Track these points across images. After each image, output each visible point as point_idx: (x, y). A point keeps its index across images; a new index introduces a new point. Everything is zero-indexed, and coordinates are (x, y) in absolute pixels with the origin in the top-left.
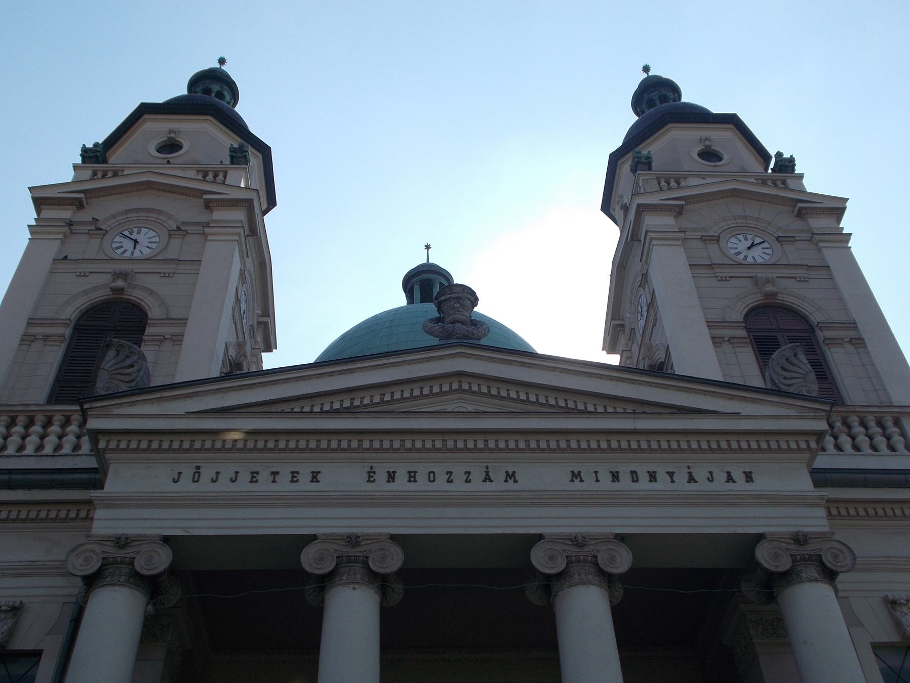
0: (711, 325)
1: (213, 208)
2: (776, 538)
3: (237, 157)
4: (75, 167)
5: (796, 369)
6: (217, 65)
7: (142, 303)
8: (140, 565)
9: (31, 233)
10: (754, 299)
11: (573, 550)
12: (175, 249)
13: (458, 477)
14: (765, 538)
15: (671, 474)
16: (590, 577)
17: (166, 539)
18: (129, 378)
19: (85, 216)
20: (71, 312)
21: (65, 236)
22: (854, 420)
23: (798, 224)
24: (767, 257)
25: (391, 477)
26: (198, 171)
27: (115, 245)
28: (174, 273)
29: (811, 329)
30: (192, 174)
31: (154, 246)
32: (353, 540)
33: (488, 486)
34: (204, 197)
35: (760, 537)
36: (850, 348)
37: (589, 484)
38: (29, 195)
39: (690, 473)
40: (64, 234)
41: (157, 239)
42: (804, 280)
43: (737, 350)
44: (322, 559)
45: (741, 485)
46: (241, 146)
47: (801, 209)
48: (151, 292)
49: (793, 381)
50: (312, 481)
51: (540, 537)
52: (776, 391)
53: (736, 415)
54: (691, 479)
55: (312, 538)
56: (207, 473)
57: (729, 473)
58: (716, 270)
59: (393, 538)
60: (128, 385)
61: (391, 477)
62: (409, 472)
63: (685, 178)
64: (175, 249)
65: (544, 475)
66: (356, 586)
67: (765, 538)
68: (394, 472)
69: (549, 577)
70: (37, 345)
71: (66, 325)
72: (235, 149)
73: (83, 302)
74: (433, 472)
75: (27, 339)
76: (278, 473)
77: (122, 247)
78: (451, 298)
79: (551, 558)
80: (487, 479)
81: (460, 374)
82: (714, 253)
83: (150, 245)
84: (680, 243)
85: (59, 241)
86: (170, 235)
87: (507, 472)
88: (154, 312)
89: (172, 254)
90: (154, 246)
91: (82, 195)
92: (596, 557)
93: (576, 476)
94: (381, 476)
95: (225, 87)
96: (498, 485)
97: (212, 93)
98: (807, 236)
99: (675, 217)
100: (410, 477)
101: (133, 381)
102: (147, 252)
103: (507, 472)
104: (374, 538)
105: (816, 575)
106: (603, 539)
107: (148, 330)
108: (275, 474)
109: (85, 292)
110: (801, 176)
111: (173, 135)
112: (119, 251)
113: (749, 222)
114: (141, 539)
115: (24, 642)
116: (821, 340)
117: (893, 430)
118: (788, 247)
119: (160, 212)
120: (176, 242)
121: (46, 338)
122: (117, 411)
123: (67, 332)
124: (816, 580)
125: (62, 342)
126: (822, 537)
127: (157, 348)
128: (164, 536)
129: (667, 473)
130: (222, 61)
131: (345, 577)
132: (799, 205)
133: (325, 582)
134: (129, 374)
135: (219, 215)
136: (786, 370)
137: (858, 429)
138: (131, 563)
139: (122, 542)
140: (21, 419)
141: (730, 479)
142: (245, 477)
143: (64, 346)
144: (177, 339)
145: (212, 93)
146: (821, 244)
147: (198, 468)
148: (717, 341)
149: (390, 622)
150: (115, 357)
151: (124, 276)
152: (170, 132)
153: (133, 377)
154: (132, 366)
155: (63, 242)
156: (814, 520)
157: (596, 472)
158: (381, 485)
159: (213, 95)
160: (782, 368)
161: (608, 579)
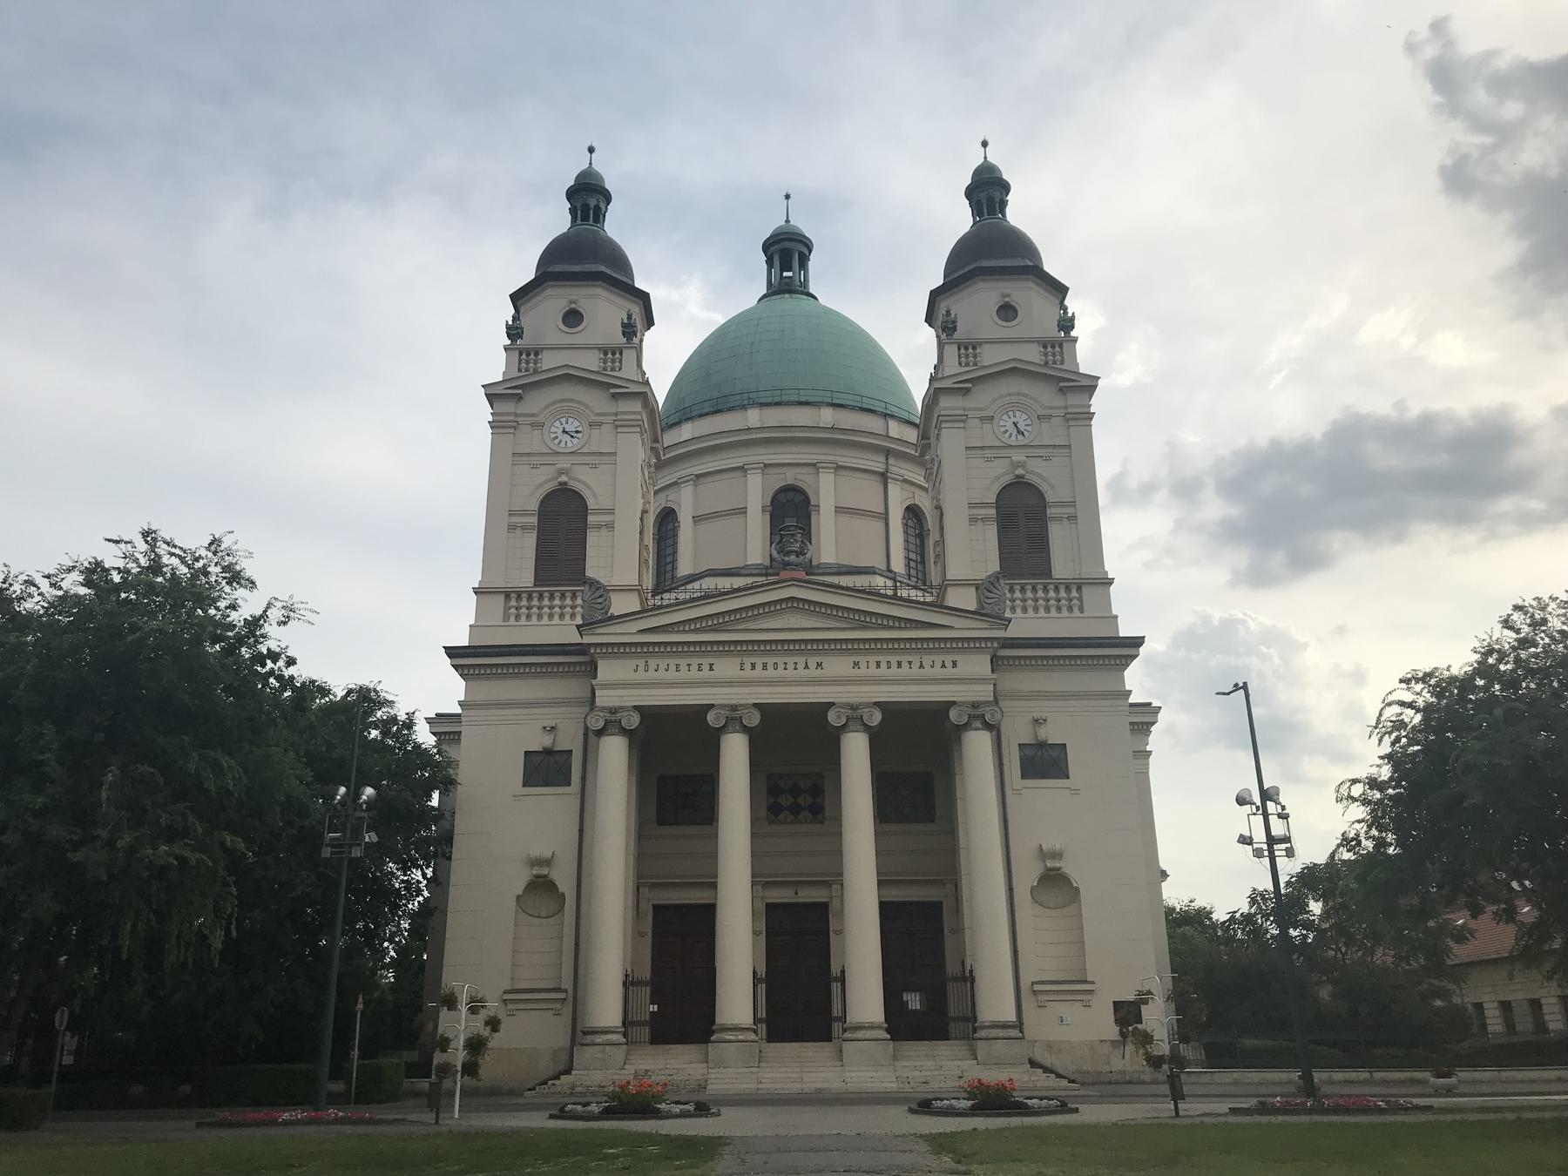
0: (972, 506)
2: (963, 704)
13: (791, 666)
17: (636, 708)
19: (523, 408)
23: (1058, 401)
32: (734, 708)
37: (863, 671)
42: (1048, 459)
45: (949, 671)
54: (921, 666)
55: (712, 706)
59: (755, 705)
61: (753, 666)
65: (838, 666)
70: (518, 531)
73: (541, 493)
75: (512, 527)
80: (806, 667)
81: (792, 599)
88: (591, 504)
93: (856, 664)
94: (748, 667)
98: (1062, 412)
104: (745, 706)
107: (591, 519)
109: (540, 485)
110: (1075, 340)
115: (562, 746)
118: (1045, 426)
119: (580, 403)
120: (595, 432)
121: (524, 528)
126: (987, 703)
133: (721, 730)
139: (613, 710)
141: (943, 666)
144: (610, 526)
156: (984, 693)
161: (867, 728)
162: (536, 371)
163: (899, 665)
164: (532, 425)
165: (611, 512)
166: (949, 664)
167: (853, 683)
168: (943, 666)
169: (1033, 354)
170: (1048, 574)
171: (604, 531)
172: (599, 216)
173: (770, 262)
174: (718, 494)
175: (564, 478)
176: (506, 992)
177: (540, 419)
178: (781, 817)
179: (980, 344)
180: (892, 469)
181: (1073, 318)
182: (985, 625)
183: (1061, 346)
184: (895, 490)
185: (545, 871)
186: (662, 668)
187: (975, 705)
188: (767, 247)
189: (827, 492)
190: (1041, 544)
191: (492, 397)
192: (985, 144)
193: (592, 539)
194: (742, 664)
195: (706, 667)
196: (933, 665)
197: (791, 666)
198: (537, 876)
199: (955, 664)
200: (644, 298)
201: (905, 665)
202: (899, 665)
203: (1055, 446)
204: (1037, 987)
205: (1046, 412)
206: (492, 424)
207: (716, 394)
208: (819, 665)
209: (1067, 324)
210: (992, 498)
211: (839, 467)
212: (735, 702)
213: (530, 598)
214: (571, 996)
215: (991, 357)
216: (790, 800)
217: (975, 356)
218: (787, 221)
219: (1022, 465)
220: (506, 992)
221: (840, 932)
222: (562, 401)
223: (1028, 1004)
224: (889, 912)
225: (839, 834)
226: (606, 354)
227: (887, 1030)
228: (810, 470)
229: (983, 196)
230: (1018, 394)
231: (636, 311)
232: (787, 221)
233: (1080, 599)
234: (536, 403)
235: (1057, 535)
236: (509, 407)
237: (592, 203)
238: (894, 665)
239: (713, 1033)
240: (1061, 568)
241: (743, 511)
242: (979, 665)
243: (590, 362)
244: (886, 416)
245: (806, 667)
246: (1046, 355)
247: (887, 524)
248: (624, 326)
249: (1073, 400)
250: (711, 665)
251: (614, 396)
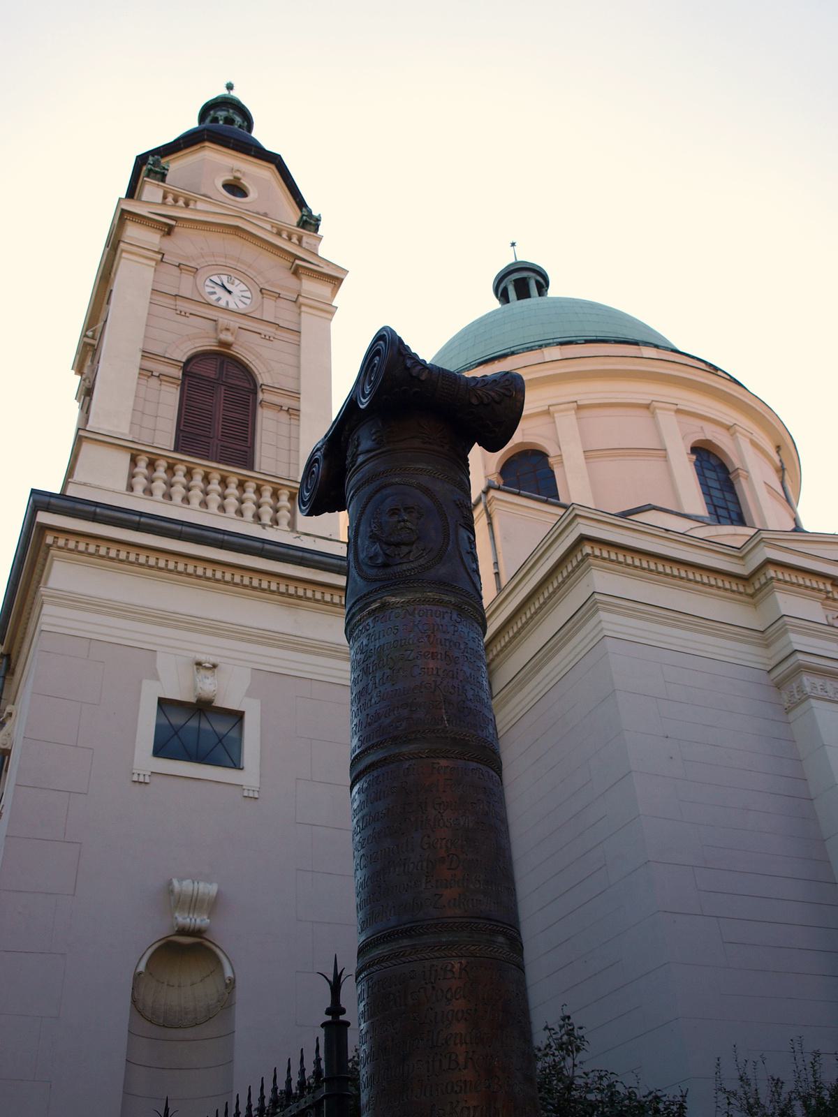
1: (303, 276)
6: (224, 92)
7: (251, 365)
12: (270, 310)
19: (168, 245)
26: (272, 227)
30: (268, 227)
31: (248, 301)
34: (298, 262)
41: (248, 294)
64: (270, 310)
70: (154, 382)
91: (173, 223)
97: (225, 124)
102: (242, 307)
111: (238, 175)
120: (269, 303)
130: (230, 87)
140: (162, 465)
145: (225, 124)
155: (155, 271)
159: (221, 122)
185: (199, 920)
198: (183, 931)
213: (171, 469)
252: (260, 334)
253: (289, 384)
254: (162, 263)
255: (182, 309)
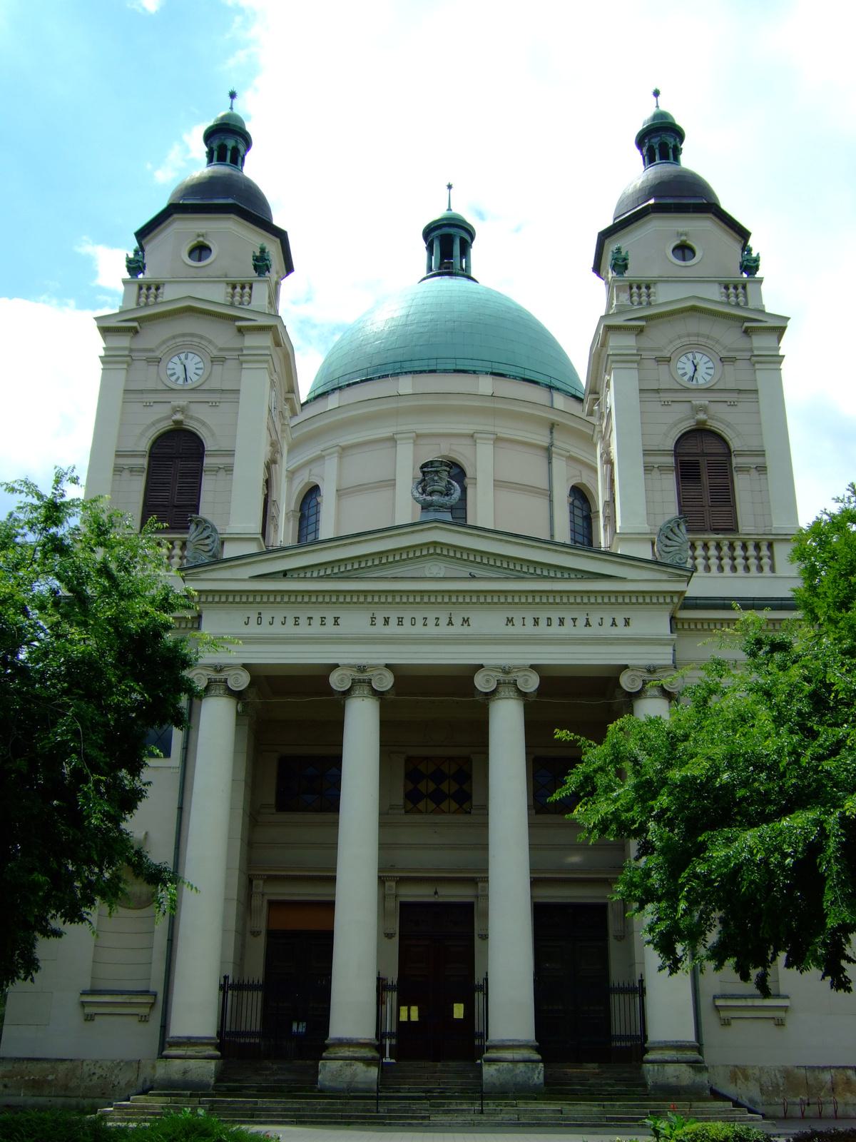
0: (647, 453)
2: (637, 668)
3: (259, 266)
4: (125, 282)
5: (676, 538)
7: (198, 433)
8: (232, 684)
9: (103, 362)
10: (687, 425)
11: (501, 676)
13: (431, 622)
14: (628, 668)
15: (574, 620)
16: (511, 693)
18: (207, 549)
20: (145, 445)
21: (129, 365)
22: (738, 545)
23: (742, 342)
24: (708, 378)
25: (386, 621)
26: (228, 284)
27: (169, 372)
28: (219, 402)
29: (728, 453)
31: (200, 372)
32: (362, 669)
33: (451, 630)
35: (626, 667)
36: (753, 472)
37: (517, 630)
38: (95, 323)
39: (587, 619)
40: (127, 362)
41: (201, 365)
42: (732, 404)
43: (664, 476)
44: (342, 680)
45: (621, 631)
46: (263, 250)
47: (747, 328)
48: (204, 424)
49: (671, 549)
50: (335, 625)
51: (481, 666)
52: (655, 562)
53: (623, 579)
54: (588, 624)
56: (266, 618)
57: (614, 619)
58: (661, 395)
59: (387, 666)
60: (209, 554)
61: (386, 621)
62: (399, 618)
63: (655, 283)
65: (488, 622)
66: (365, 699)
67: (628, 668)
68: (388, 618)
69: (486, 694)
70: (126, 474)
71: (143, 456)
72: (257, 257)
73: (153, 433)
74: (414, 618)
75: (118, 470)
76: (312, 618)
77: (174, 374)
78: (431, 471)
79: (488, 681)
80: (450, 623)
81: (435, 544)
82: (662, 377)
83: (198, 372)
84: (635, 365)
85: (124, 372)
86: (212, 361)
87: (464, 618)
88: (209, 445)
89: (214, 384)
90: (200, 372)
91: (135, 324)
92: (516, 680)
93: (510, 621)
94: (380, 621)
95: (240, 140)
96: (457, 629)
99: (637, 335)
100: (401, 621)
101: (210, 550)
103: (464, 618)
104: (375, 667)
105: (656, 693)
106: (520, 668)
107: (207, 461)
108: (310, 618)
109: (153, 424)
111: (201, 239)
112: (174, 378)
113: (700, 339)
114: (230, 666)
116: (734, 465)
117: (765, 552)
118: (729, 368)
119: (201, 337)
120: (218, 368)
121: (132, 470)
122: (203, 576)
123: (144, 462)
124: (655, 697)
125: (143, 472)
126: (664, 668)
127: (214, 477)
128: (244, 664)
129: (572, 619)
131: (357, 692)
132: (747, 324)
133: (347, 693)
134: (207, 545)
135: (251, 341)
136: (670, 540)
137: (739, 552)
138: (226, 681)
139: (219, 669)
141: (614, 624)
142: (290, 621)
143: (145, 475)
144: (229, 469)
146: (757, 366)
147: (260, 614)
148: (648, 469)
149: (387, 726)
150: (196, 530)
151: (182, 410)
152: (199, 236)
153: (210, 548)
154: (208, 537)
156: (662, 656)
157: (524, 618)
158: (380, 629)
160: (667, 537)
161: (522, 695)
162: (156, 304)
163: (562, 622)
164: (149, 361)
165: (231, 453)
166: (620, 622)
167: (506, 645)
168: (614, 624)
169: (713, 294)
170: (733, 529)
171: (222, 474)
172: (236, 159)
173: (430, 248)
174: (365, 467)
175: (178, 417)
176: (84, 993)
177: (158, 354)
178: (421, 805)
179: (655, 283)
180: (556, 442)
181: (757, 260)
182: (664, 577)
183: (744, 287)
184: (559, 465)
186: (278, 622)
187: (651, 670)
188: (429, 232)
189: (483, 465)
190: (725, 496)
191: (106, 331)
192: (656, 94)
193: (208, 483)
194: (373, 619)
195: (330, 621)
196: (602, 623)
197: (431, 622)
199: (627, 622)
200: (281, 235)
201: (568, 622)
202: (562, 622)
203: (740, 391)
204: (719, 1002)
205: (732, 354)
206: (105, 360)
207: (369, 365)
208: (466, 621)
209: (750, 266)
210: (670, 444)
211: (498, 440)
212: (364, 662)
214: (159, 1002)
215: (666, 296)
216: (432, 786)
217: (649, 296)
218: (449, 209)
219: (704, 409)
220: (84, 993)
221: (485, 937)
222: (184, 335)
223: (709, 1018)
224: (544, 916)
225: (485, 825)
226: (234, 288)
227: (538, 1050)
228: (468, 441)
229: (655, 141)
230: (698, 335)
231: (273, 250)
232: (449, 209)
233: (771, 558)
234: (153, 337)
235: (743, 485)
236: (124, 341)
237: (230, 143)
238: (555, 622)
239: (326, 1047)
240: (747, 522)
241: (391, 483)
242: (658, 624)
243: (216, 295)
244: (551, 388)
245: (450, 623)
246: (728, 296)
247: (551, 501)
248: (256, 259)
249: (760, 342)
250: (336, 619)
251: (241, 330)
252: (208, 402)
253: (225, 445)
254: (135, 362)
255: (148, 400)
